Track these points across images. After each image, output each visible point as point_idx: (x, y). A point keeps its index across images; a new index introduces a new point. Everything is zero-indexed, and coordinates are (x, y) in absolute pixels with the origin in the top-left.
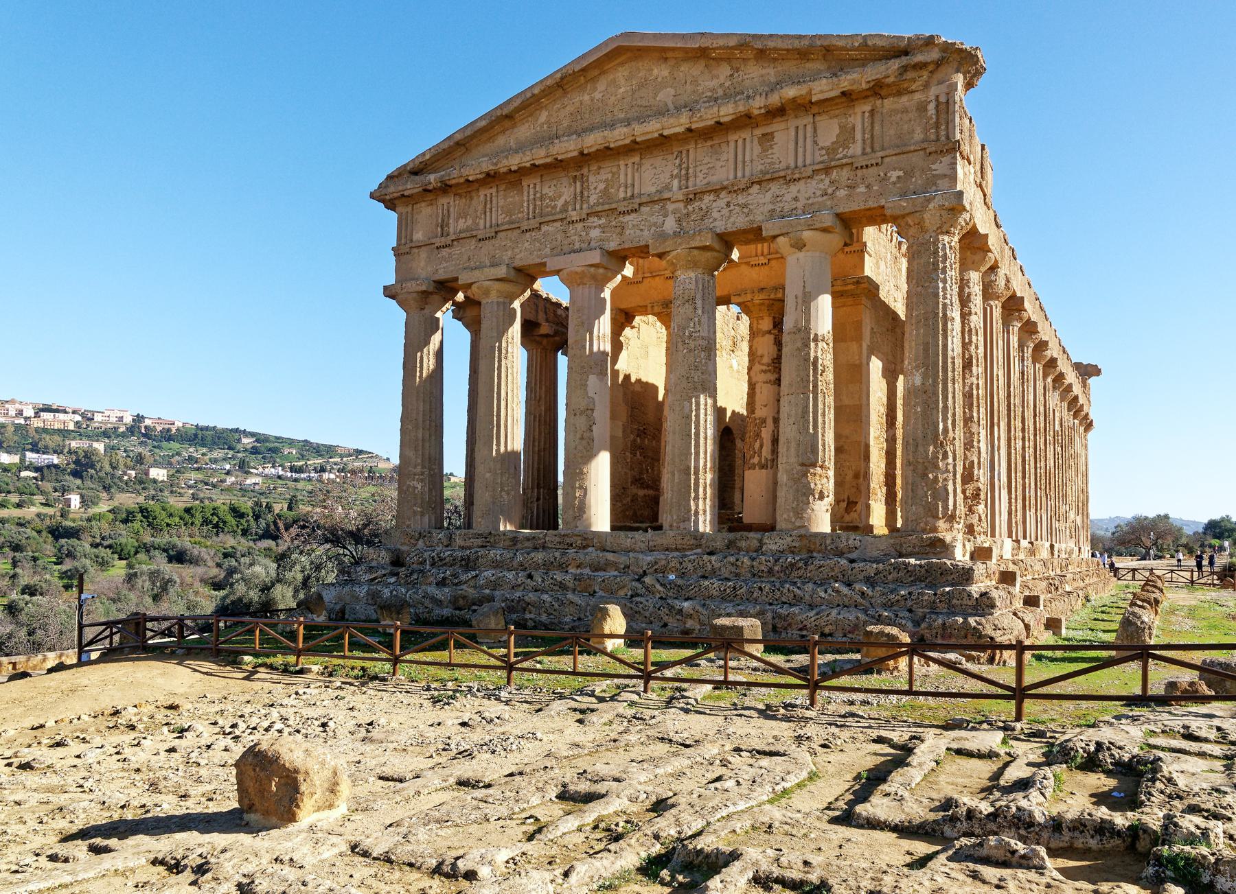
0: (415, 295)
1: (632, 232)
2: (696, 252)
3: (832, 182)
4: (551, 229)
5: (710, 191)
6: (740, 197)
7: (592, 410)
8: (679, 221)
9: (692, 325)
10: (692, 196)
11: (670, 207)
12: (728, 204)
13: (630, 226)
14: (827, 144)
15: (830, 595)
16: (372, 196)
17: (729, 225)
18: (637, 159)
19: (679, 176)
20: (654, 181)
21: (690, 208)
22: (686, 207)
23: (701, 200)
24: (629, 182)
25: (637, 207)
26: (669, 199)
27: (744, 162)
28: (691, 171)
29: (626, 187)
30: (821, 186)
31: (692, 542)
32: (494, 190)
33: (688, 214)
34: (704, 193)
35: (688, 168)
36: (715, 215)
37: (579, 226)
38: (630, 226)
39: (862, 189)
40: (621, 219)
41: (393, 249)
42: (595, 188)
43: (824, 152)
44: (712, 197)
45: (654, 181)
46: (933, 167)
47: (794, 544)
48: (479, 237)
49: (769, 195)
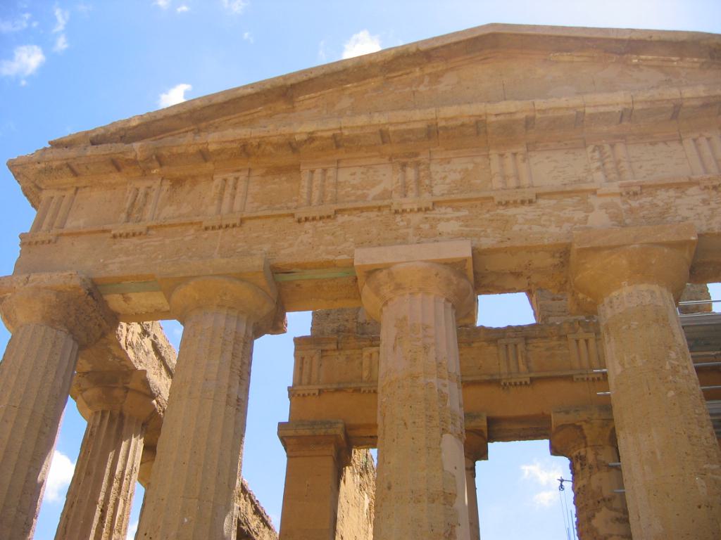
1: (526, 227)
5: (667, 186)
16: (12, 165)
18: (522, 149)
21: (634, 204)
22: (625, 202)
29: (505, 178)
32: (242, 176)
37: (416, 218)
40: (501, 211)
41: (22, 236)
44: (672, 193)
48: (205, 224)
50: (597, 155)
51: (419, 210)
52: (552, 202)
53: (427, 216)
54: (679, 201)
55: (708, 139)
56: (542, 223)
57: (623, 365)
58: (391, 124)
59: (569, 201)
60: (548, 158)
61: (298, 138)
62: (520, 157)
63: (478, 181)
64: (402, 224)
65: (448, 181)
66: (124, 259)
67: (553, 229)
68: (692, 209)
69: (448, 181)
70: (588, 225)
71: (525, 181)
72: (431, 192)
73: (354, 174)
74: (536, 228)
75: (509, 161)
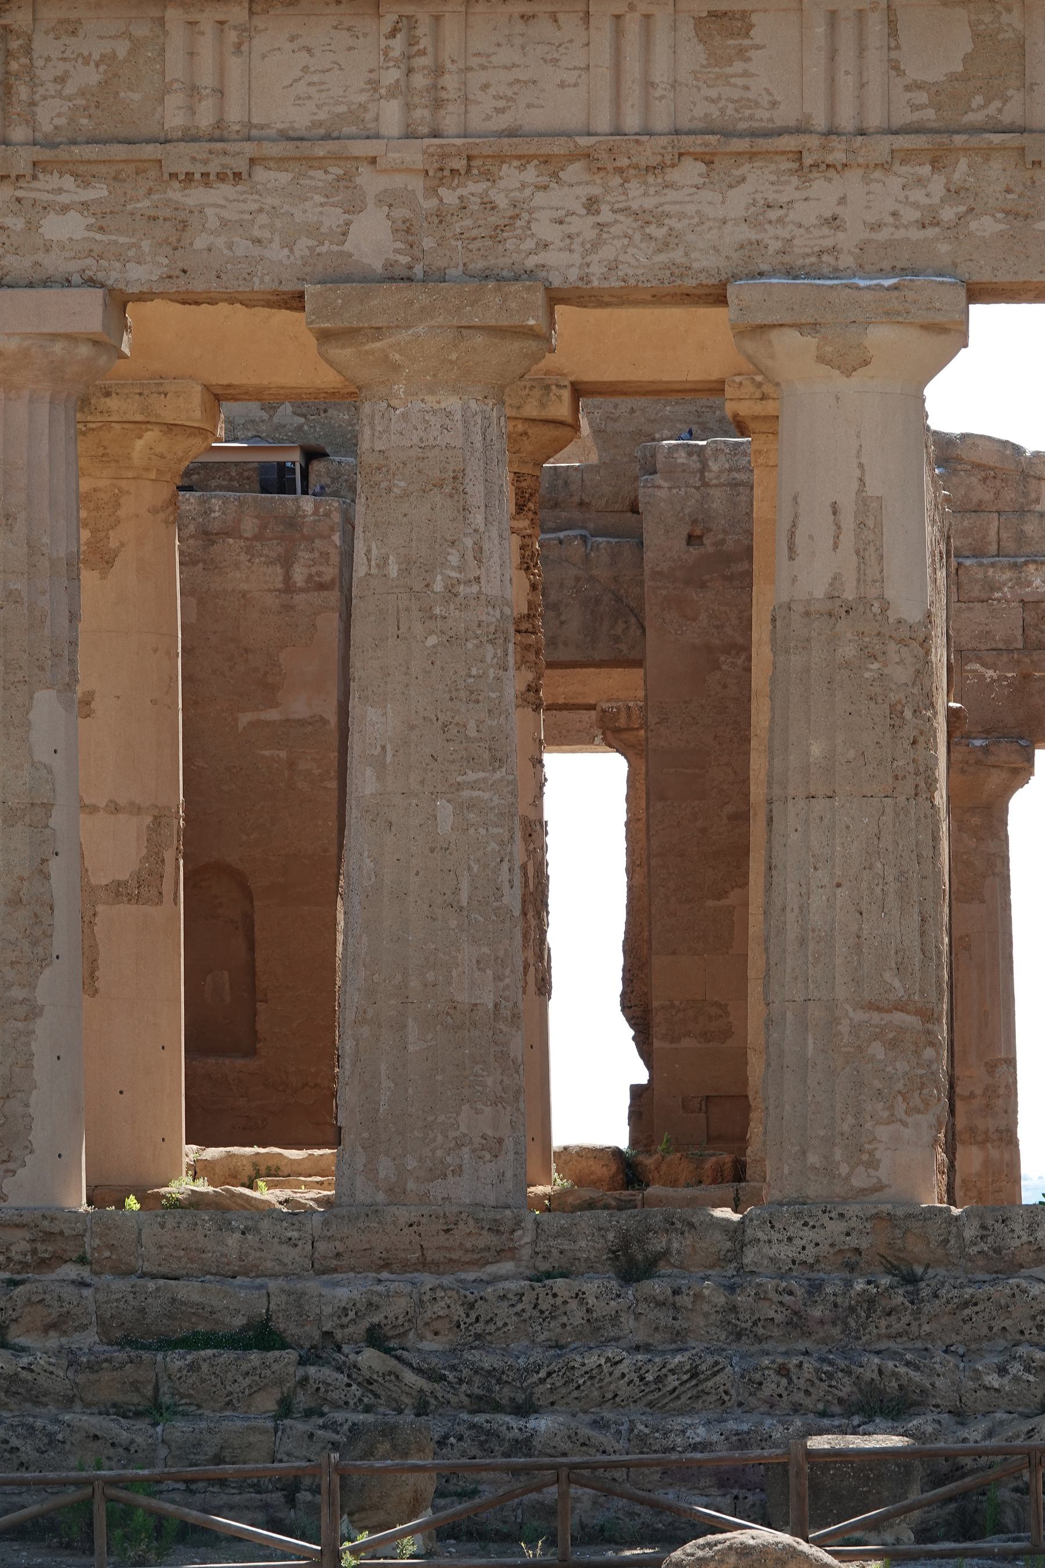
1: (220, 242)
2: (479, 339)
3: (954, 193)
5: (525, 159)
6: (635, 188)
7: (48, 807)
8: (406, 230)
9: (454, 559)
10: (460, 164)
11: (369, 181)
12: (592, 205)
13: (213, 223)
14: (935, 75)
15: (1016, 1379)
17: (596, 270)
20: (301, 88)
21: (449, 197)
22: (432, 191)
23: (489, 176)
24: (207, 79)
25: (242, 166)
27: (648, 85)
28: (450, 81)
29: (193, 91)
30: (917, 195)
31: (486, 1239)
33: (440, 216)
35: (439, 70)
36: (544, 229)
38: (213, 223)
40: (175, 193)
42: (61, 80)
44: (531, 174)
45: (301, 88)
47: (853, 1241)
49: (738, 201)
50: (398, 45)
52: (284, 177)
53: (19, 193)
54: (540, 199)
55: (647, 17)
56: (256, 233)
57: (369, 560)
60: (292, 39)
62: (232, 36)
63: (136, 96)
67: (276, 253)
68: (561, 223)
69: (70, 89)
70: (347, 247)
71: (234, 115)
72: (32, 122)
74: (243, 247)
75: (206, 45)
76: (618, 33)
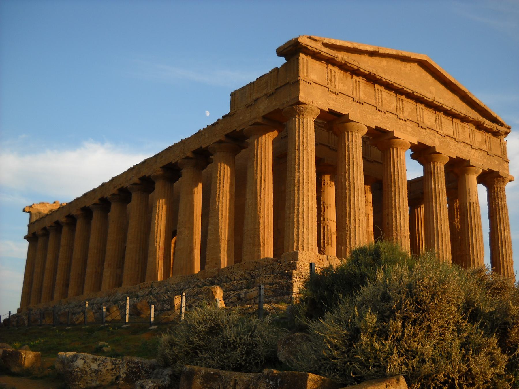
0: (319, 110)
4: (390, 116)
10: (445, 135)
12: (455, 145)
14: (479, 141)
19: (439, 125)
21: (443, 139)
26: (437, 132)
28: (443, 125)
30: (480, 155)
34: (448, 136)
35: (441, 123)
36: (451, 146)
37: (403, 122)
38: (423, 134)
39: (489, 162)
40: (419, 128)
42: (407, 109)
43: (478, 143)
45: (429, 120)
46: (504, 165)
51: (404, 120)
52: (429, 131)
55: (458, 124)
58: (405, 87)
59: (432, 132)
61: (384, 80)
64: (400, 123)
65: (408, 111)
66: (334, 103)
73: (387, 96)
74: (426, 139)
75: (421, 110)
76: (456, 125)
